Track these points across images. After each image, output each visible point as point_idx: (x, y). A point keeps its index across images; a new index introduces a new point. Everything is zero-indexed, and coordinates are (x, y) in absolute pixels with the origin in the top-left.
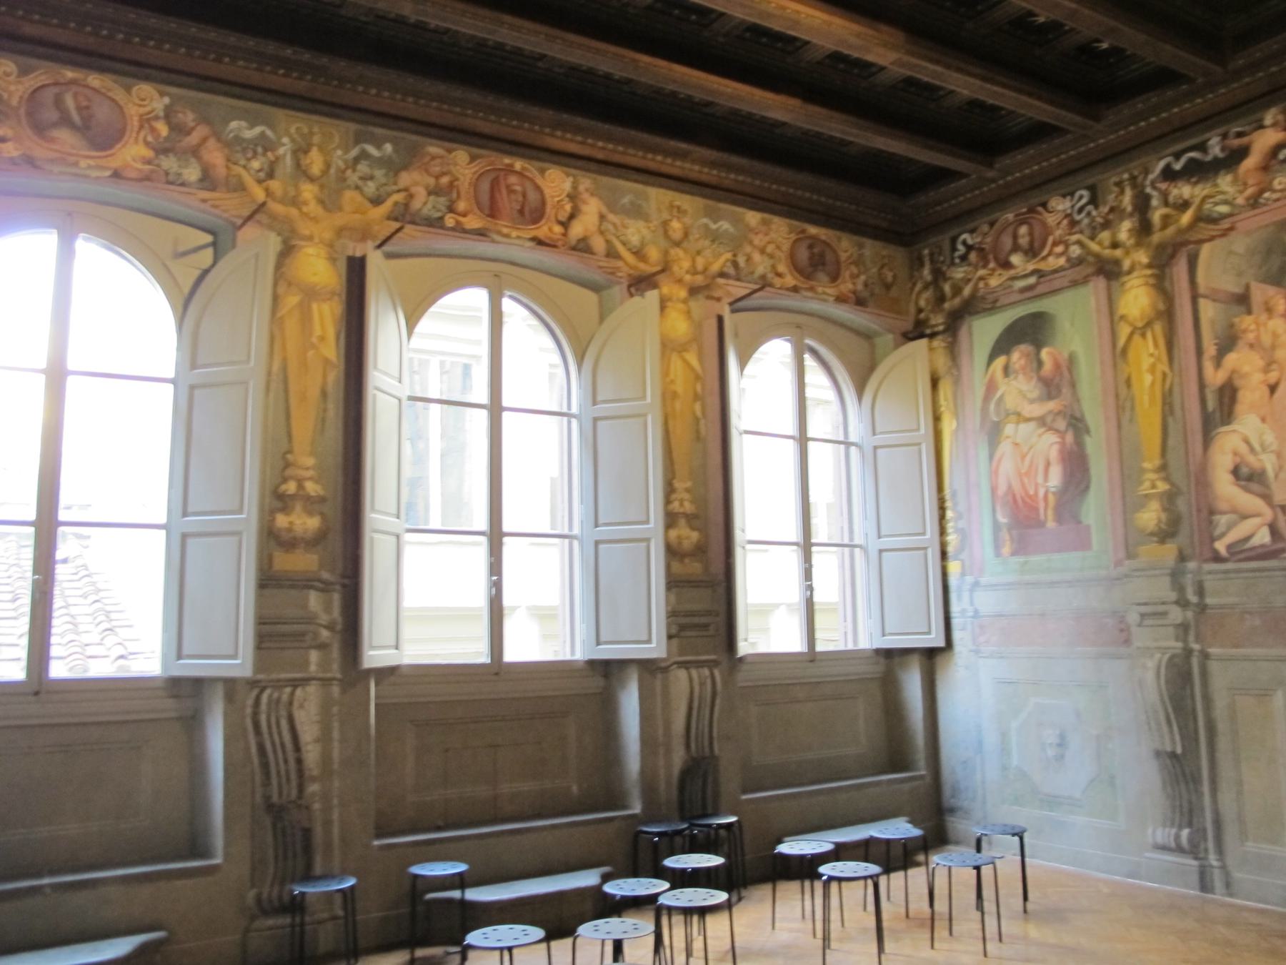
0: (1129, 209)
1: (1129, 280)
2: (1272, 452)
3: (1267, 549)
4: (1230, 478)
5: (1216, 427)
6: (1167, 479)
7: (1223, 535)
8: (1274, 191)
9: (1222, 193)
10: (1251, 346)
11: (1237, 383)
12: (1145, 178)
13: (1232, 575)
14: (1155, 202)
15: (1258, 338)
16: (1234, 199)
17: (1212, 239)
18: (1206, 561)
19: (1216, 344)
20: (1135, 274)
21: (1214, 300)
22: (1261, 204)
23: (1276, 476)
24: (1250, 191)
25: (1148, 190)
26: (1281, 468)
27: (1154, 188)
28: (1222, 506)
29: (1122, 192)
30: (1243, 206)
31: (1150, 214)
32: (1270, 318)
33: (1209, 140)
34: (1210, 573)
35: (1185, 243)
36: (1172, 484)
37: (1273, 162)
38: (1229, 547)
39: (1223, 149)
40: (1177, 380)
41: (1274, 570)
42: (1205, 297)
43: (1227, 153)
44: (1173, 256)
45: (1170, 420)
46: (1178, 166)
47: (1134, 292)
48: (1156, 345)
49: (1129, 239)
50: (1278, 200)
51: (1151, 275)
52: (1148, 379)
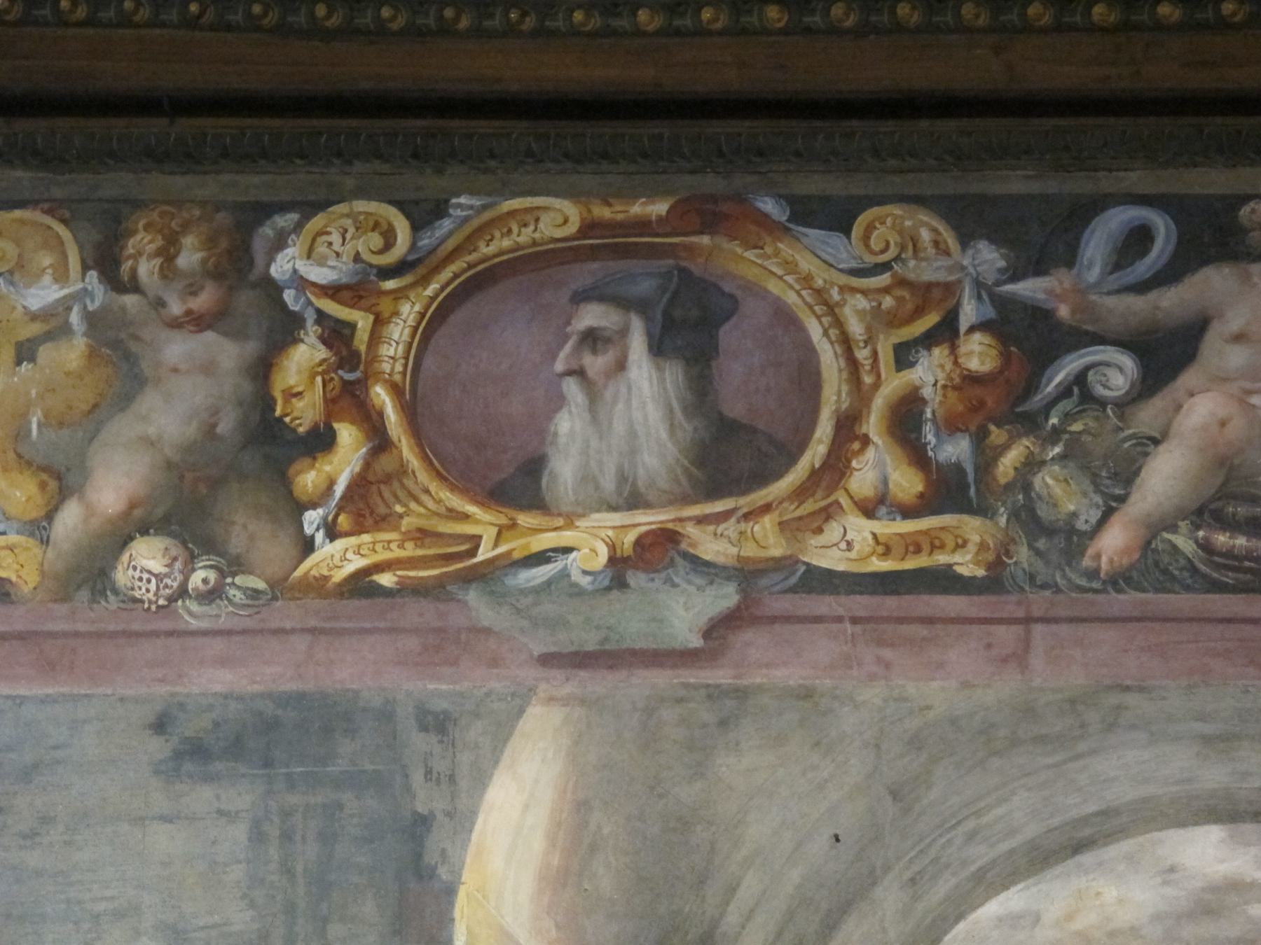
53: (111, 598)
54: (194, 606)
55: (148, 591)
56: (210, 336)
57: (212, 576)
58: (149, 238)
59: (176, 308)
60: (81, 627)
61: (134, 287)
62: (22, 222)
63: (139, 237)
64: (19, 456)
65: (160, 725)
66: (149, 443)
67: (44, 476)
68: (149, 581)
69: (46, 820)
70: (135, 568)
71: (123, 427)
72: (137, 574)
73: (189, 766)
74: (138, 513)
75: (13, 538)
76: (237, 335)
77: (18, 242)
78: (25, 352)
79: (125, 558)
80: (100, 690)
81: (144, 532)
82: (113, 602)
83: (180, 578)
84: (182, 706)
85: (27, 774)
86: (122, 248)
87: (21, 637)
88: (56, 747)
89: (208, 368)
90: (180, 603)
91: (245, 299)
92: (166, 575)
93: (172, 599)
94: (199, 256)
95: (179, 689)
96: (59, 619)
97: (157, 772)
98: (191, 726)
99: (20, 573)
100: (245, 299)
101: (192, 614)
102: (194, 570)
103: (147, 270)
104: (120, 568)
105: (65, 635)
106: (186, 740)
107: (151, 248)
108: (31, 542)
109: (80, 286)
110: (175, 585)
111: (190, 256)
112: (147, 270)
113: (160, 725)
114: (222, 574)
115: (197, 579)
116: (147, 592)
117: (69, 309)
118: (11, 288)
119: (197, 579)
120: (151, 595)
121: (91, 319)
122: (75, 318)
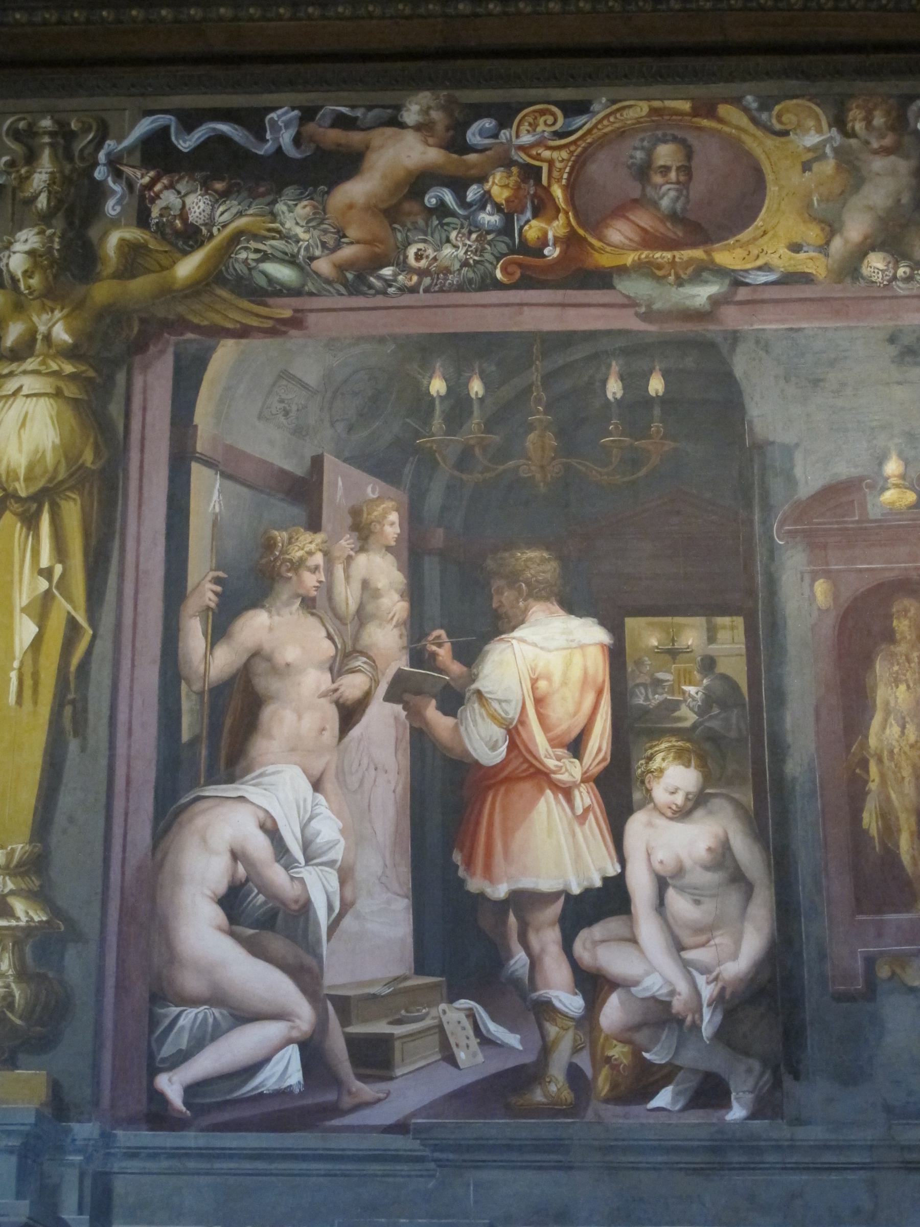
0: (42, 202)
1: (11, 374)
2: (331, 864)
3: (289, 1105)
4: (216, 914)
5: (195, 783)
6: (40, 897)
7: (182, 1057)
8: (403, 266)
9: (283, 236)
10: (308, 604)
11: (264, 683)
12: (99, 144)
13: (192, 1164)
14: (111, 208)
15: (328, 588)
16: (312, 258)
17: (243, 333)
18: (131, 1122)
19: (217, 581)
20: (31, 364)
21: (225, 476)
22: (371, 286)
23: (333, 927)
24: (347, 252)
25: (99, 174)
26: (346, 906)
27: (118, 174)
28: (192, 983)
29: (31, 158)
30: (328, 281)
31: (93, 233)
32: (362, 549)
33: (274, 109)
34: (133, 1154)
35: (180, 325)
36: (55, 911)
37: (407, 206)
38: (192, 1091)
39: (297, 141)
40: (104, 647)
41: (303, 1158)
42: (209, 463)
43: (308, 151)
44: (139, 346)
45: (73, 745)
46: (186, 144)
47: (19, 406)
48: (60, 551)
49: (27, 274)
50: (413, 290)
51: (73, 377)
52: (26, 630)
53: (861, 281)
54: (900, 284)
55: (878, 278)
56: (893, 158)
57: (908, 270)
58: (858, 112)
59: (875, 145)
60: (849, 295)
61: (853, 135)
62: (798, 105)
63: (854, 111)
64: (810, 215)
65: (892, 340)
66: (870, 208)
67: (823, 225)
68: (878, 273)
69: (843, 385)
70: (871, 267)
71: (856, 201)
72: (872, 270)
73: (907, 359)
74: (869, 241)
75: (812, 254)
76: (906, 157)
77: (796, 115)
78: (806, 167)
79: (866, 262)
80: (861, 324)
81: (873, 249)
82: (862, 283)
83: (892, 271)
84: (901, 331)
85: (832, 363)
86: (847, 116)
87: (821, 300)
88: (843, 351)
89: (894, 172)
90: (894, 283)
91: (907, 140)
92: (886, 270)
93: (890, 281)
94: (882, 120)
95: (899, 323)
96: (838, 291)
97: (893, 362)
98: (907, 340)
99: (818, 270)
100: (907, 140)
101: (901, 288)
102: (898, 268)
103: (859, 126)
104: (864, 267)
105: (842, 298)
106: (906, 347)
107: (861, 116)
108: (821, 256)
109: (829, 135)
110: (891, 274)
111: (879, 120)
112: (859, 126)
113: (892, 340)
114: (912, 269)
115: (901, 272)
116: (878, 278)
117: (825, 146)
118: (796, 137)
119: (901, 272)
120: (880, 280)
121: (837, 151)
122: (828, 150)
